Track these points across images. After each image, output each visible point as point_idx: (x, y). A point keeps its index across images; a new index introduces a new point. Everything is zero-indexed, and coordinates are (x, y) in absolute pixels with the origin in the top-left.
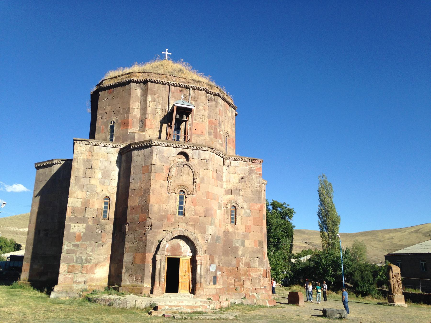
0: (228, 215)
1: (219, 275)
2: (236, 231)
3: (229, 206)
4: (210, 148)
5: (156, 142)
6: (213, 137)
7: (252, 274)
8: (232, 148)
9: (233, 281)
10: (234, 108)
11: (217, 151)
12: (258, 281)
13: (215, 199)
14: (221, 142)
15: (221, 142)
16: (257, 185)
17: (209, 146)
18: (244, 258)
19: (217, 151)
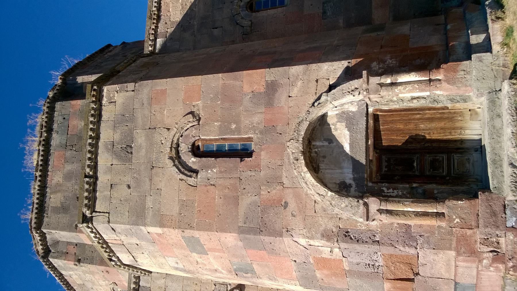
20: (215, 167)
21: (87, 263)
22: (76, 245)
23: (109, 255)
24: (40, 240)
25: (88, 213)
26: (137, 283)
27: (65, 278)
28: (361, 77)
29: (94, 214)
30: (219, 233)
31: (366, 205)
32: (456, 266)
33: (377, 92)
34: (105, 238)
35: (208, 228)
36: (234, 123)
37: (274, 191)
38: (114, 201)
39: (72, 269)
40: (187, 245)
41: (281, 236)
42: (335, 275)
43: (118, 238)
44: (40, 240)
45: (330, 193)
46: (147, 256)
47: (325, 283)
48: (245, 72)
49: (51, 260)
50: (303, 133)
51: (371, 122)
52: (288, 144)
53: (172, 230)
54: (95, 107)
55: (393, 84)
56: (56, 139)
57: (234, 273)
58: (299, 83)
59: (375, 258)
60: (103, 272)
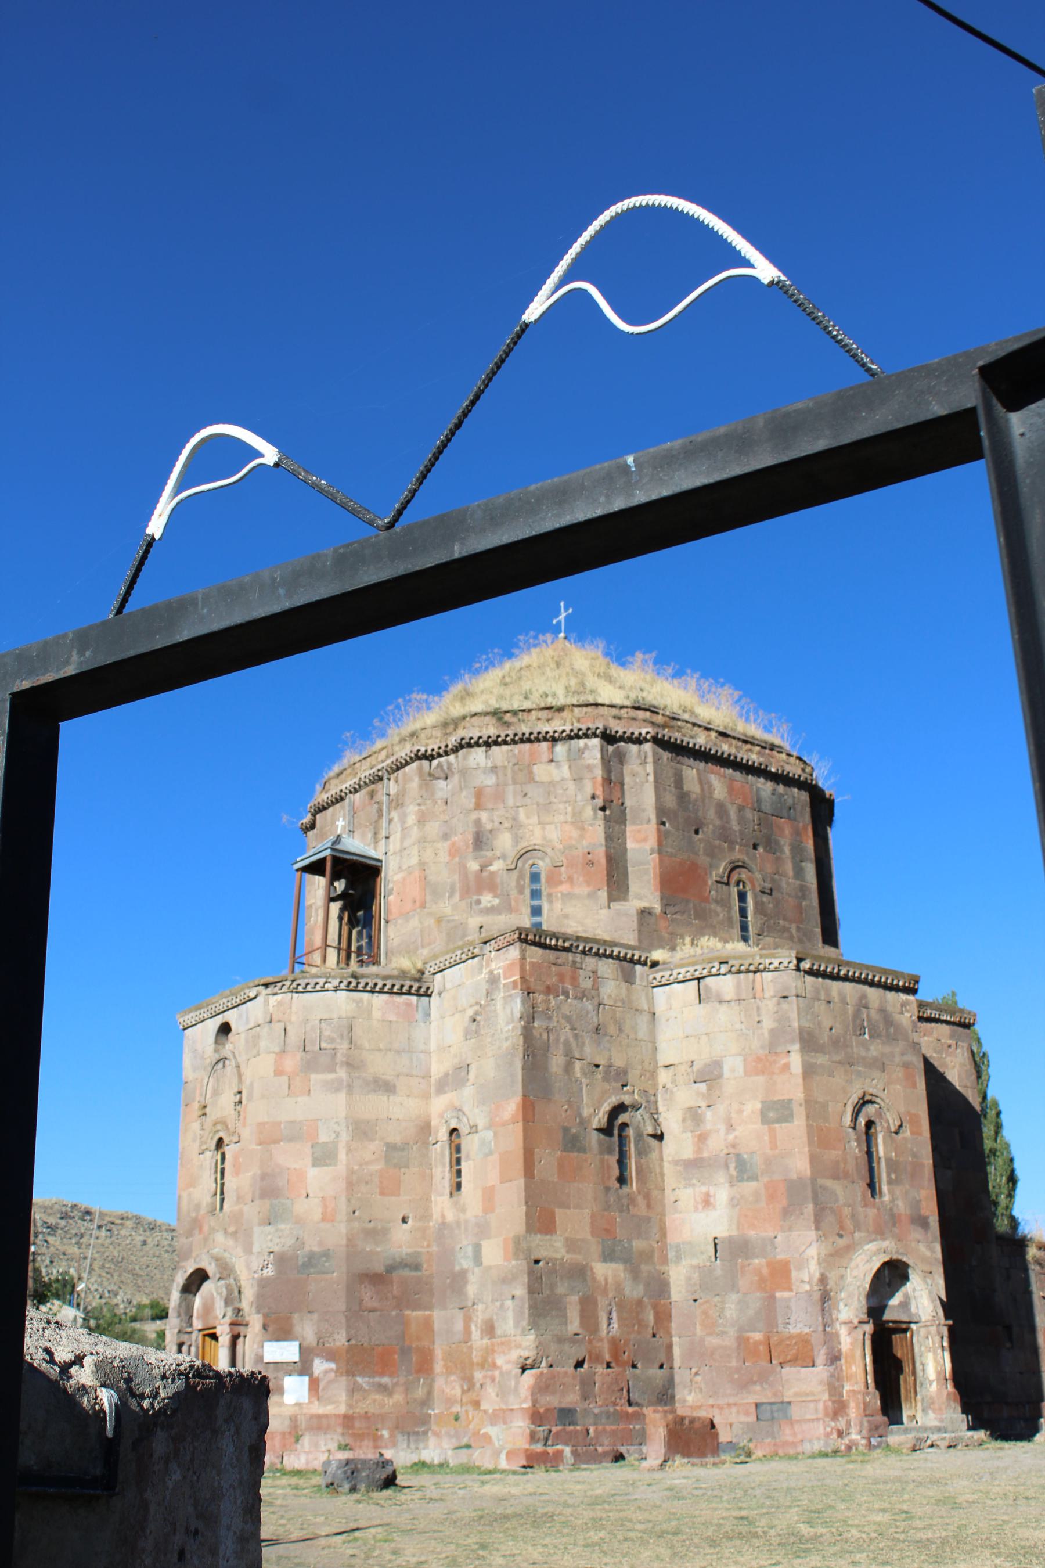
0: (444, 1165)
1: (326, 1372)
2: (461, 1215)
3: (443, 1135)
4: (263, 985)
5: (181, 1020)
6: (457, 896)
7: (499, 1361)
8: (583, 890)
9: (458, 1391)
10: (586, 736)
11: (294, 985)
12: (513, 1383)
13: (291, 1139)
14: (496, 901)
15: (496, 901)
16: (506, 1029)
17: (257, 983)
18: (480, 1307)
19: (295, 984)
20: (860, 1151)
21: (605, 828)
22: (622, 804)
23: (732, 966)
24: (633, 733)
25: (806, 965)
26: (639, 962)
27: (545, 745)
28: (947, 1317)
29: (802, 973)
30: (807, 1155)
31: (868, 1322)
32: (815, 1401)
33: (939, 1333)
34: (764, 974)
35: (810, 1143)
36: (896, 1177)
37: (848, 1222)
38: (816, 1004)
39: (578, 780)
40: (775, 1102)
41: (817, 1228)
42: (762, 1280)
43: (767, 995)
44: (633, 733)
45: (867, 1286)
46: (738, 1026)
47: (743, 1267)
48: (934, 1192)
49: (596, 742)
50: (905, 1259)
51: (904, 1326)
52: (893, 1243)
53: (801, 1088)
54: (901, 984)
55: (943, 1347)
56: (766, 787)
57: (732, 1150)
58: (928, 1253)
59: (800, 1325)
60: (589, 853)
